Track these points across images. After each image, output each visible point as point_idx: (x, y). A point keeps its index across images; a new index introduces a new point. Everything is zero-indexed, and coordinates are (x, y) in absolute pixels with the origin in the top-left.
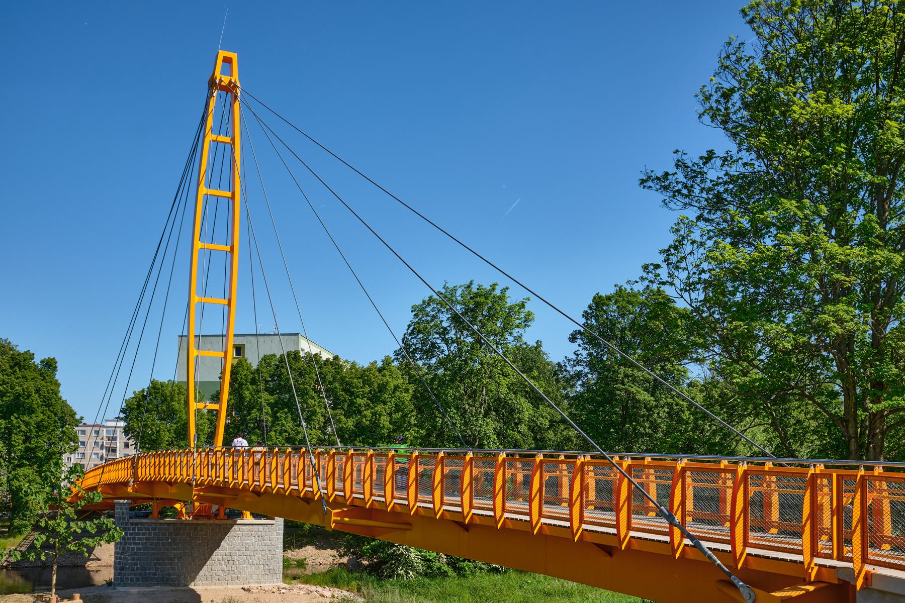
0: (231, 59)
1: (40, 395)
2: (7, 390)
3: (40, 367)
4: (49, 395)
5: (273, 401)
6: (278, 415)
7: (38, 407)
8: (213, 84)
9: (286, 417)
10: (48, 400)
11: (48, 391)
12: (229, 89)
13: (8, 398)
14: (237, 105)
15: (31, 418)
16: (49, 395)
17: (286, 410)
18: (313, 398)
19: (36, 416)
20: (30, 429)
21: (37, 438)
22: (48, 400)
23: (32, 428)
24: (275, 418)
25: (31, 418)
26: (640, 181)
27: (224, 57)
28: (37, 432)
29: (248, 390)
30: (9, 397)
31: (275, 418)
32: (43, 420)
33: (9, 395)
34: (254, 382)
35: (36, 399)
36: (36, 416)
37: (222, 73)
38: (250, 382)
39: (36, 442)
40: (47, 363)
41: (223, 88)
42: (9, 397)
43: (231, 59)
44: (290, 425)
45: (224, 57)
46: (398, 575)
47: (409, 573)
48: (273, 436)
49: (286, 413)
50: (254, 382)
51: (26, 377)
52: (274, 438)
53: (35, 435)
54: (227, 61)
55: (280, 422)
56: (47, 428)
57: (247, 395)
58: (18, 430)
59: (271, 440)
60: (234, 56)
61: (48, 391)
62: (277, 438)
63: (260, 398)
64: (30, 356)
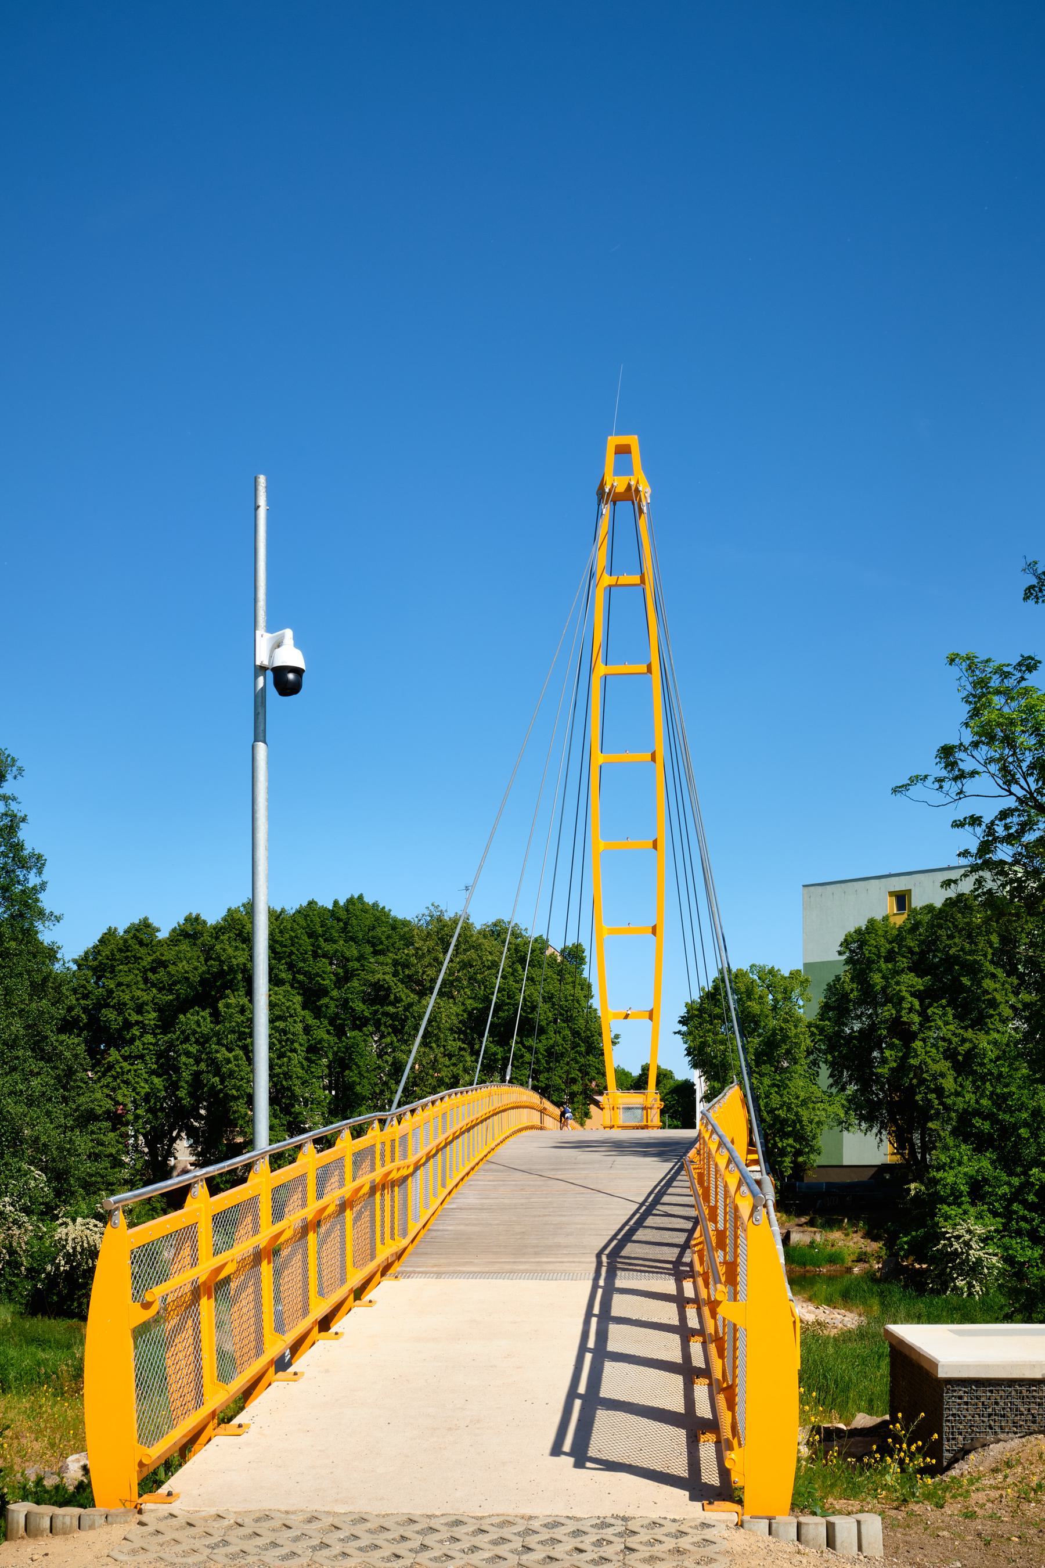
0: (629, 446)
1: (554, 1004)
2: (503, 1001)
3: (559, 959)
4: (567, 1004)
5: (922, 988)
6: (929, 1011)
7: (547, 1024)
8: (601, 494)
9: (945, 1015)
10: (567, 1011)
11: (566, 997)
12: (631, 494)
13: (506, 1013)
14: (643, 523)
15: (540, 1041)
16: (567, 1004)
17: (944, 1001)
18: (993, 976)
19: (547, 1038)
20: (538, 1060)
21: (548, 1072)
22: (567, 1011)
23: (541, 1057)
24: (926, 1018)
25: (540, 1041)
26: (16, 758)
27: (617, 446)
28: (548, 1063)
29: (881, 971)
30: (508, 1011)
31: (926, 1018)
32: (556, 1044)
33: (506, 1008)
34: (890, 957)
35: (543, 1013)
36: (547, 1038)
37: (617, 472)
38: (885, 957)
39: (547, 1079)
40: (569, 954)
41: (616, 499)
42: (508, 1011)
43: (629, 446)
44: (951, 1027)
45: (617, 446)
46: (955, 1288)
47: (974, 1286)
48: (919, 1049)
49: (944, 1007)
50: (890, 957)
51: (533, 978)
52: (920, 1051)
53: (545, 1067)
54: (623, 451)
55: (932, 1024)
56: (562, 1055)
57: (877, 981)
58: (520, 1061)
59: (916, 1056)
60: (632, 440)
61: (566, 997)
62: (926, 1053)
63: (898, 983)
64: (542, 944)
